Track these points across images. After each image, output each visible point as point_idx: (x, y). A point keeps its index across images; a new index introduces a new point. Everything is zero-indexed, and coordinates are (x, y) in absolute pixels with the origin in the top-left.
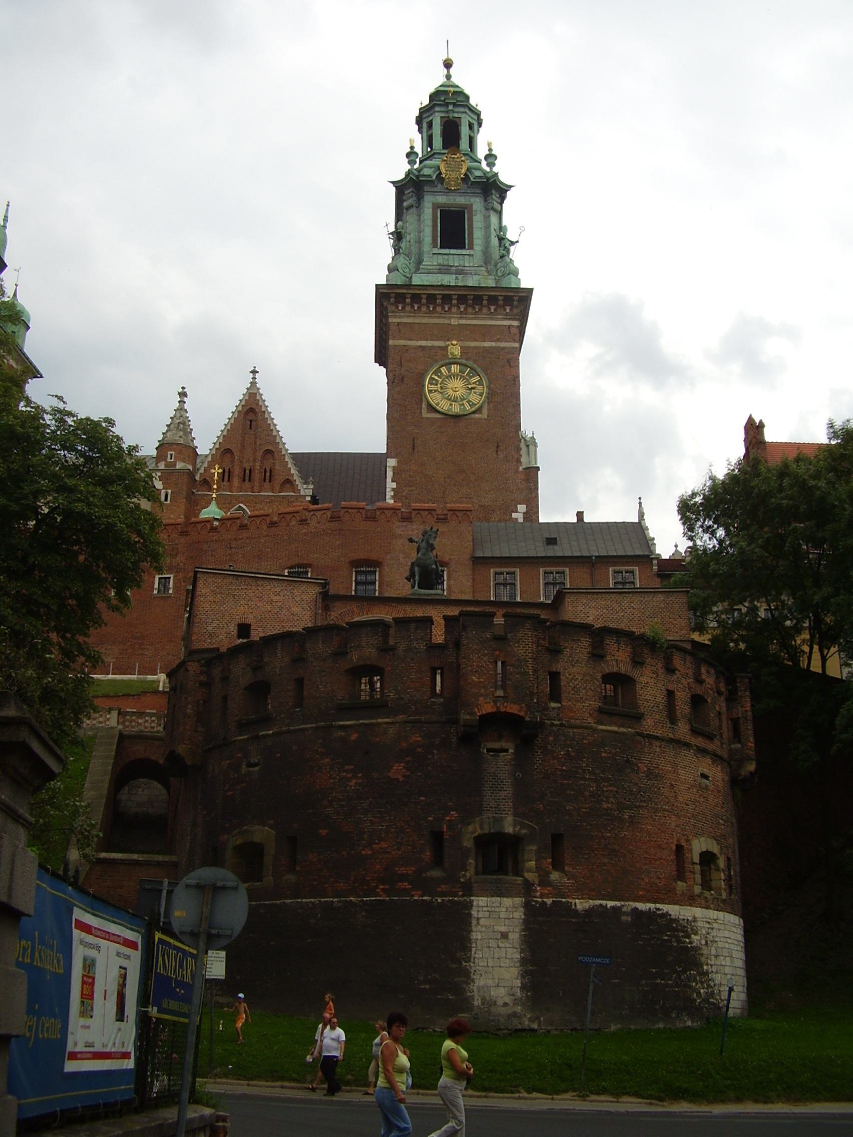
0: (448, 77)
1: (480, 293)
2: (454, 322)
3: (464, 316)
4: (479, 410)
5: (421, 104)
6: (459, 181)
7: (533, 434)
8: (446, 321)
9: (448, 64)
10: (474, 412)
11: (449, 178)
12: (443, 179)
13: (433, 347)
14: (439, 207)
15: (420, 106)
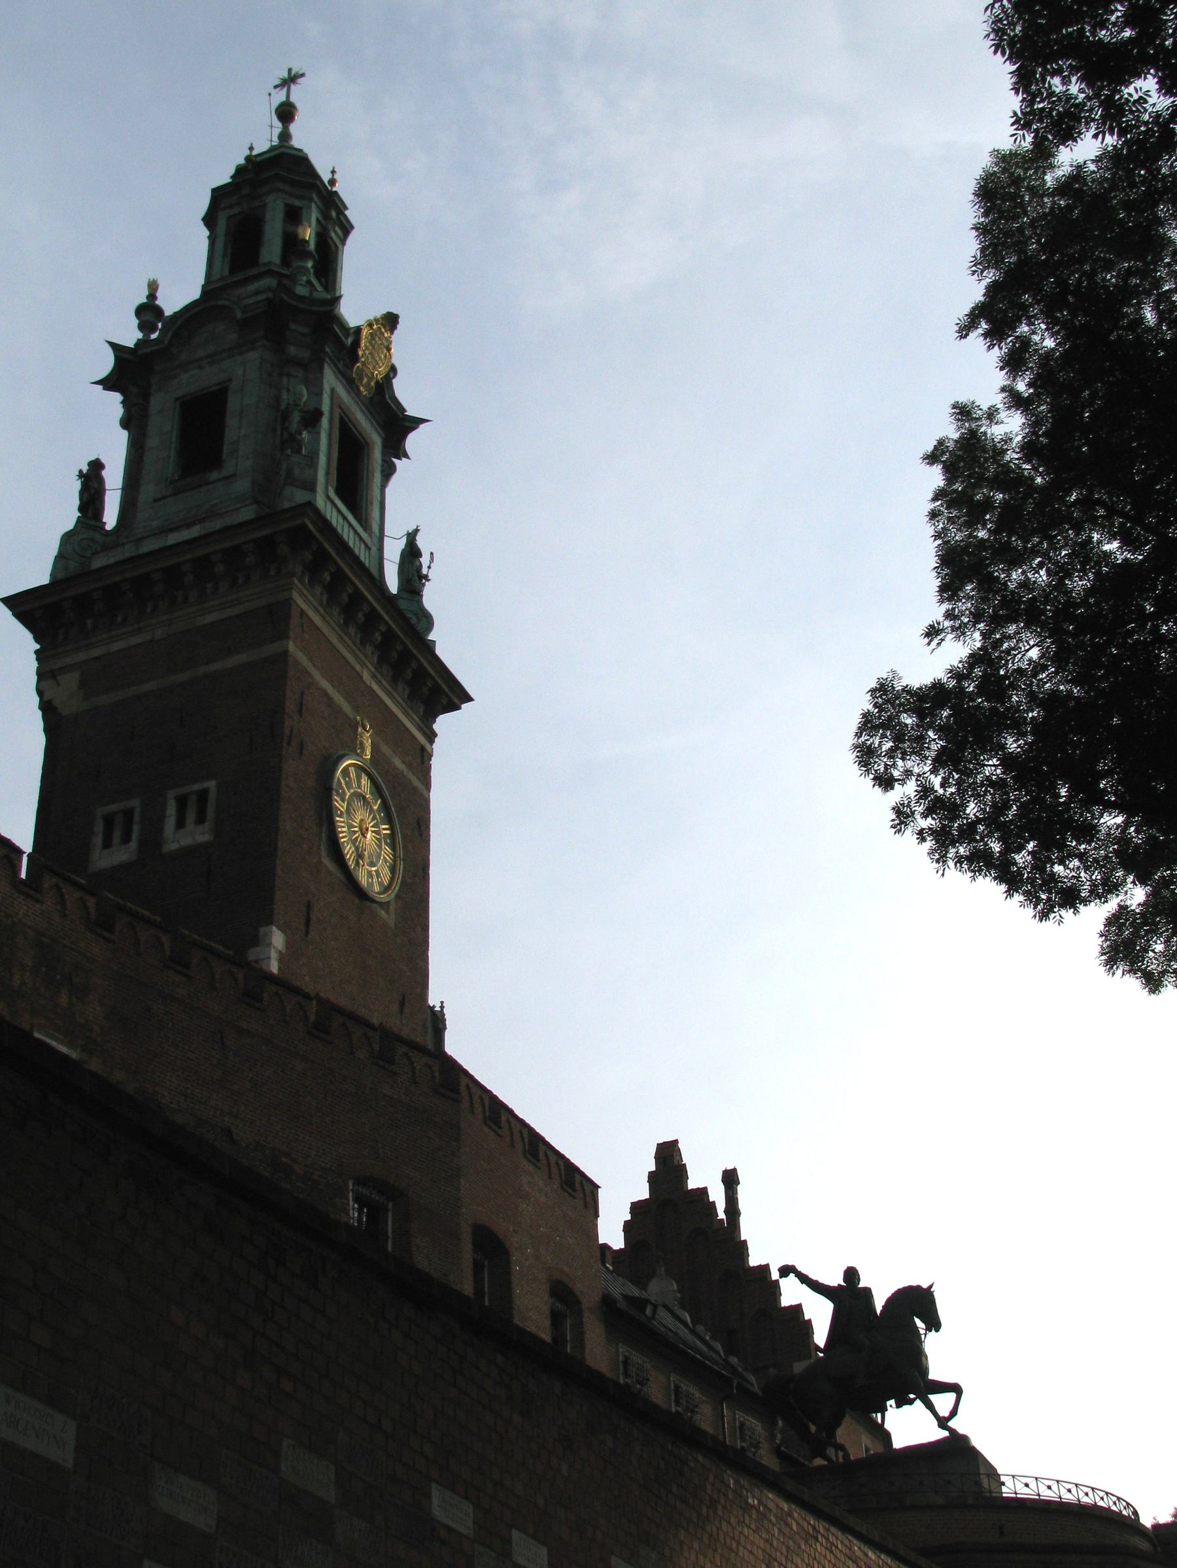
0: (285, 136)
1: (415, 652)
2: (366, 676)
3: (379, 676)
4: (385, 905)
5: (251, 149)
6: (373, 384)
7: (442, 1007)
8: (358, 667)
9: (286, 113)
10: (381, 904)
11: (364, 364)
12: (355, 358)
13: (338, 711)
14: (340, 407)
15: (247, 152)
